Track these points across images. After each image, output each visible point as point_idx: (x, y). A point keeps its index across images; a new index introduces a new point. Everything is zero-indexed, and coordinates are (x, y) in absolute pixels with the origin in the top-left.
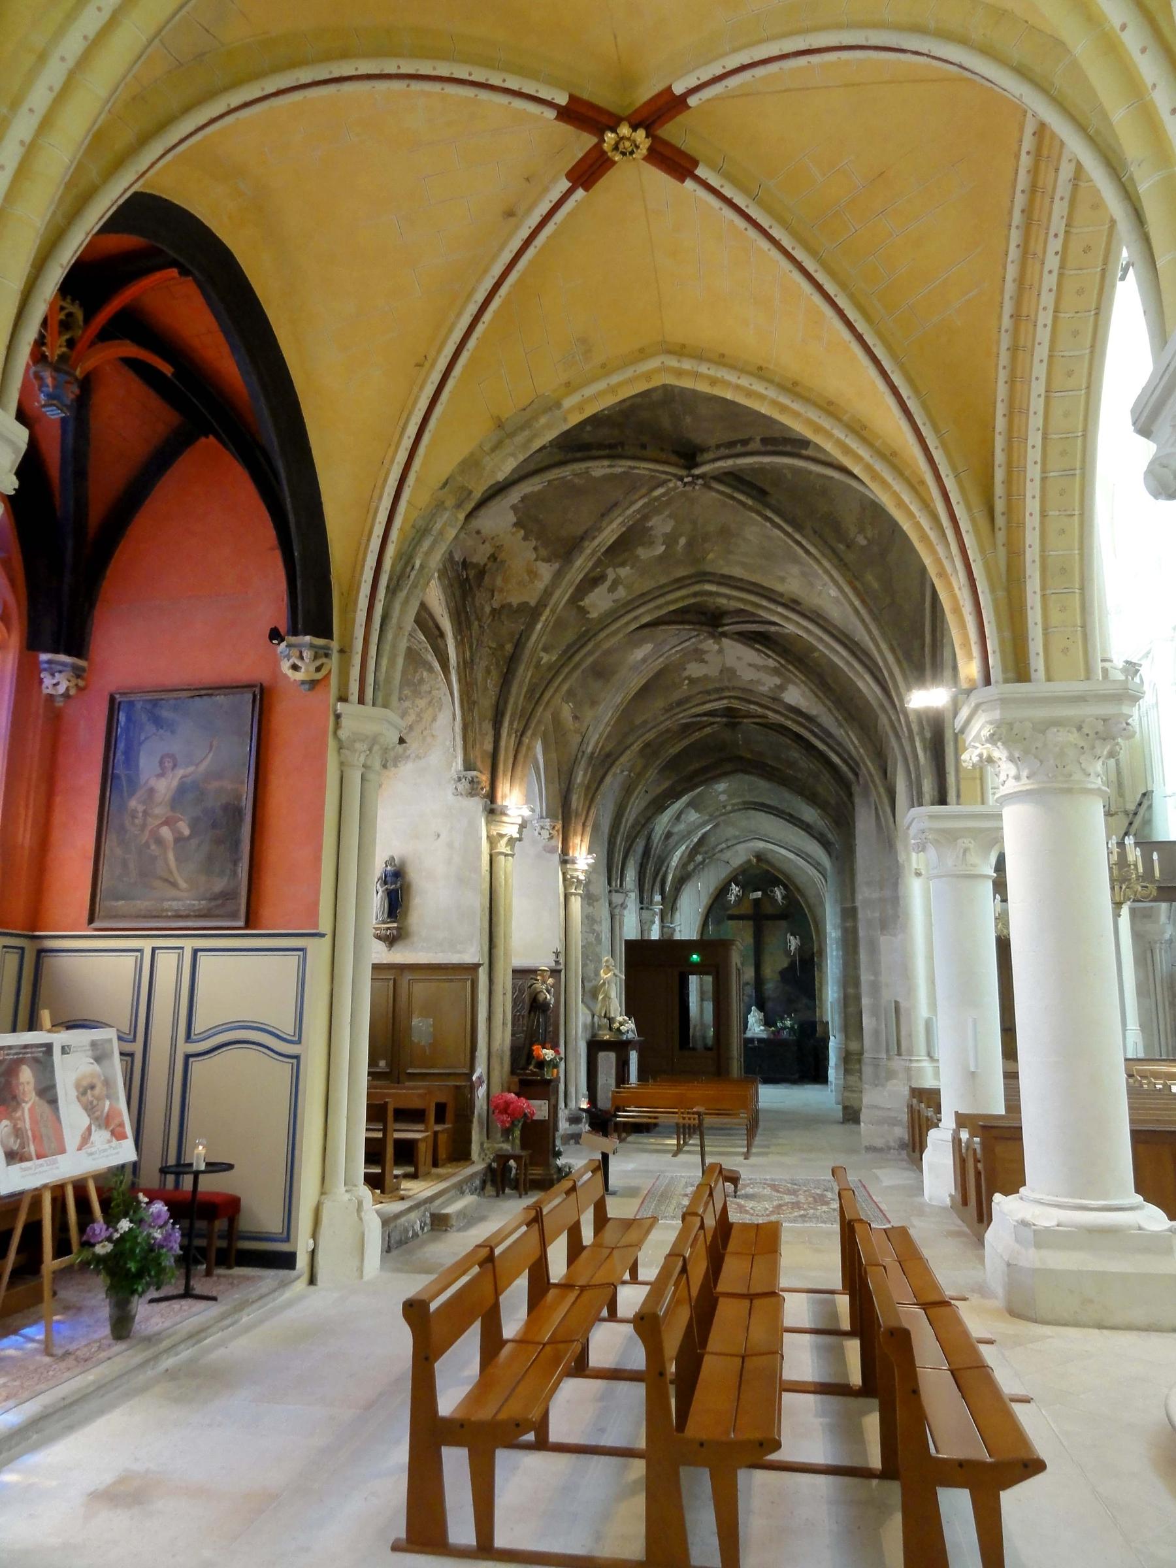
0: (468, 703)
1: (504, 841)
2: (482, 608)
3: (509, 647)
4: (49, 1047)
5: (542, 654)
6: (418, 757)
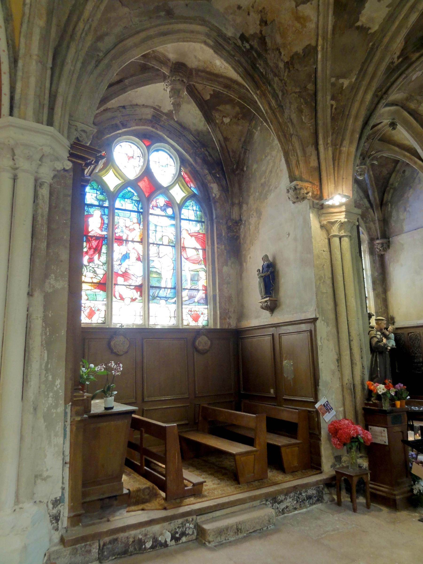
0: (285, 138)
1: (337, 226)
2: (277, 67)
3: (310, 86)
5: (341, 81)
6: (276, 188)
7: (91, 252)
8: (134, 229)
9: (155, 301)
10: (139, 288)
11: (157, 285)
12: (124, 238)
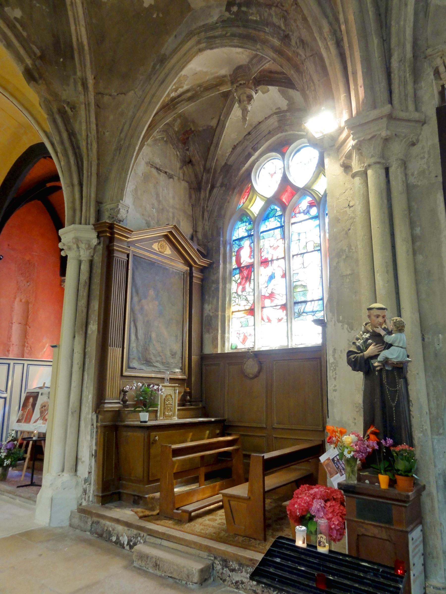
4: (38, 393)
7: (244, 282)
8: (278, 246)
9: (301, 317)
10: (284, 307)
11: (303, 299)
12: (270, 259)
